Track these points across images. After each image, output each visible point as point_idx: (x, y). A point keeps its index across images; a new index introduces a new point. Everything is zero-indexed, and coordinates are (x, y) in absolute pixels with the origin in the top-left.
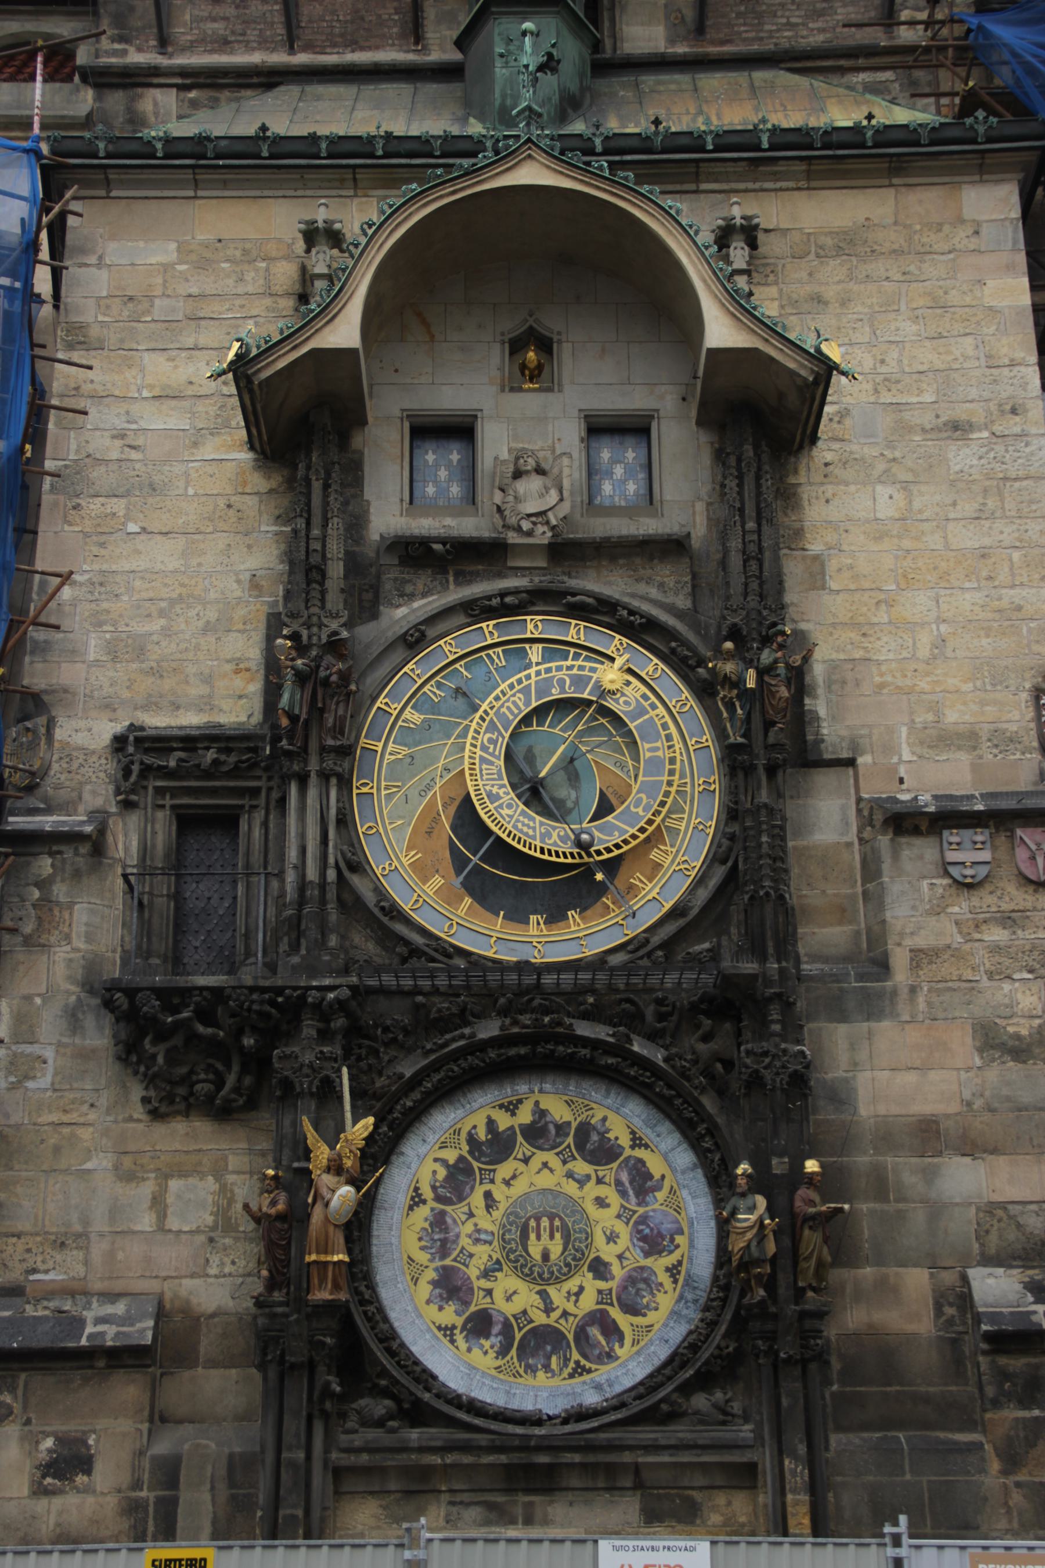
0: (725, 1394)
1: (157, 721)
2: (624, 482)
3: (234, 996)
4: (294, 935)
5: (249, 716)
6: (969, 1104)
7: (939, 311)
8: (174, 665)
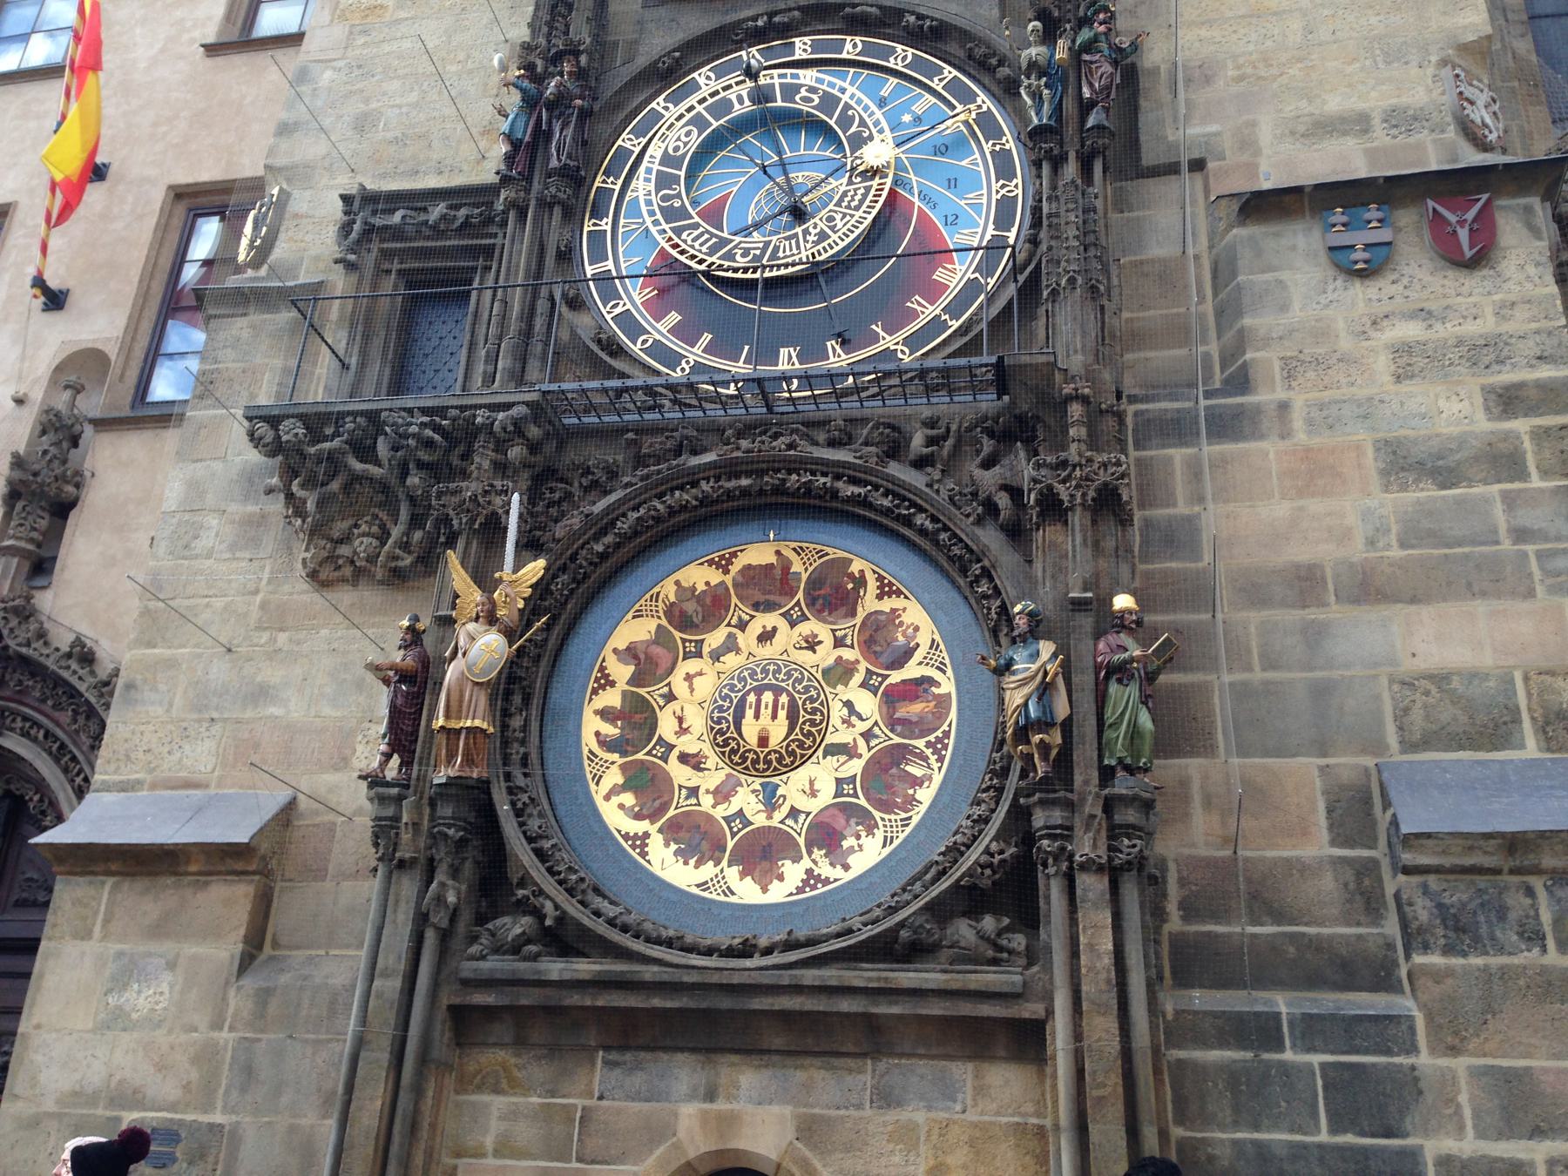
0: (998, 920)
3: (391, 420)
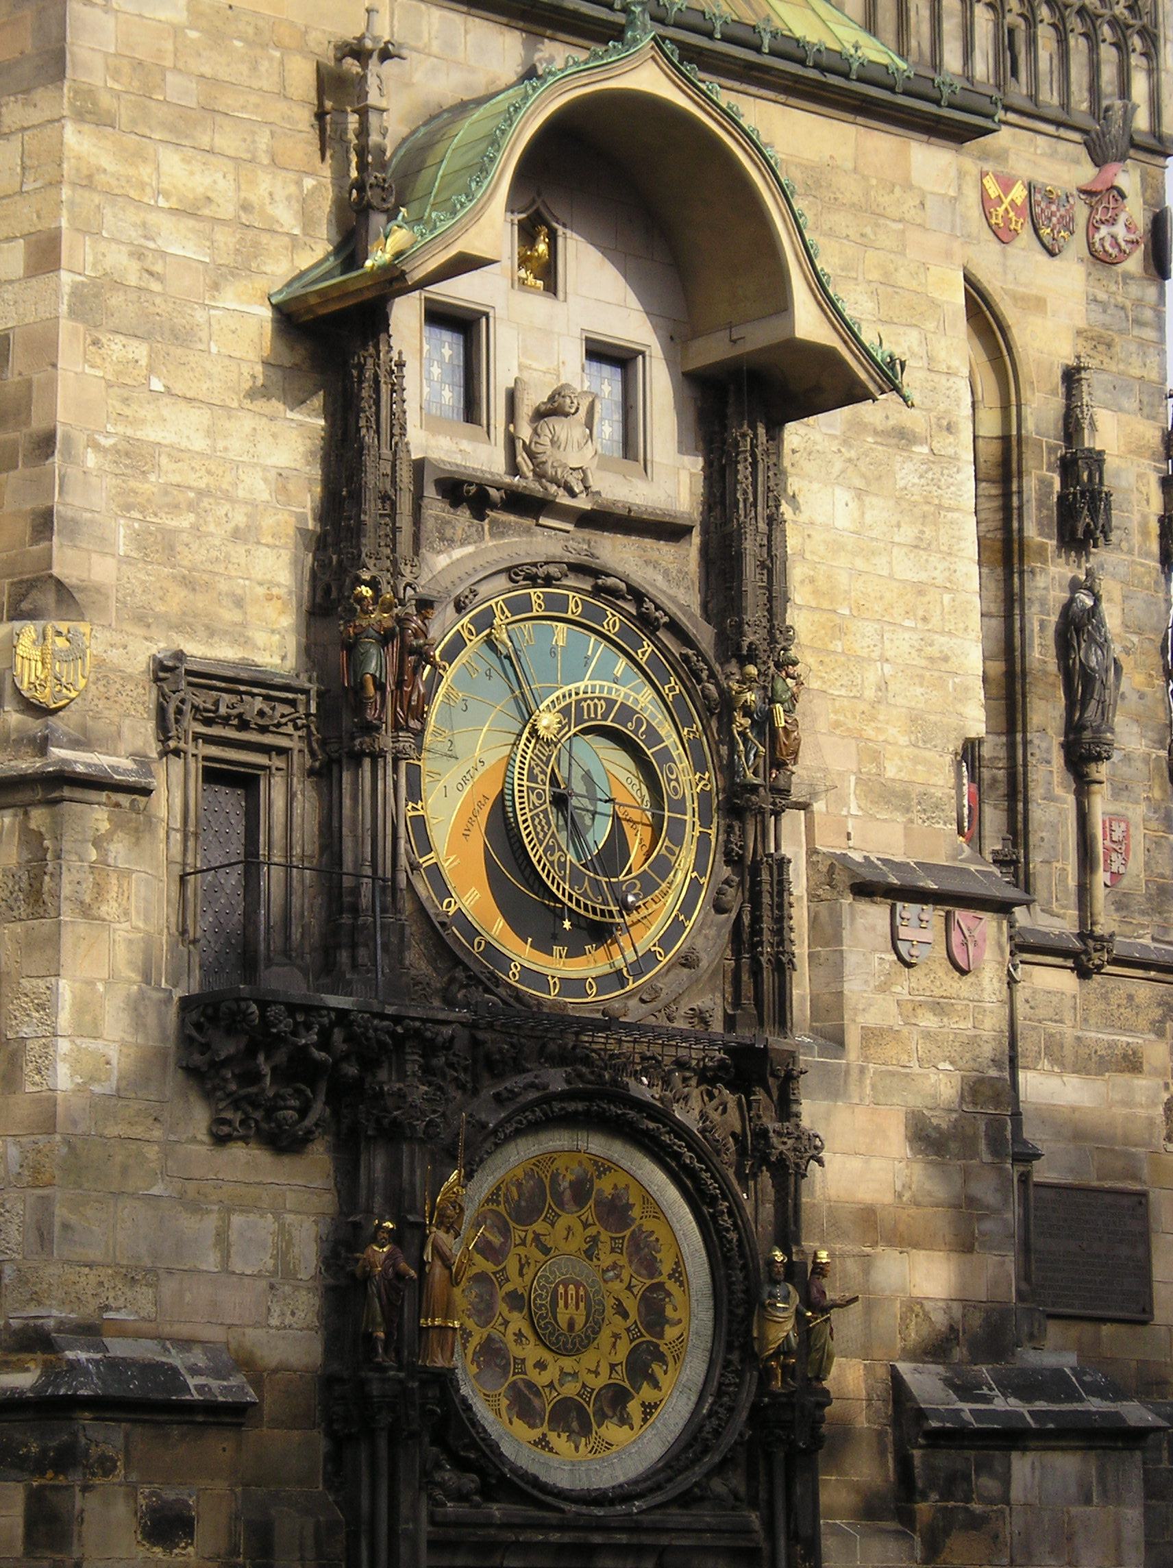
5: (283, 658)
6: (900, 1196)
7: (890, 289)
8: (206, 577)
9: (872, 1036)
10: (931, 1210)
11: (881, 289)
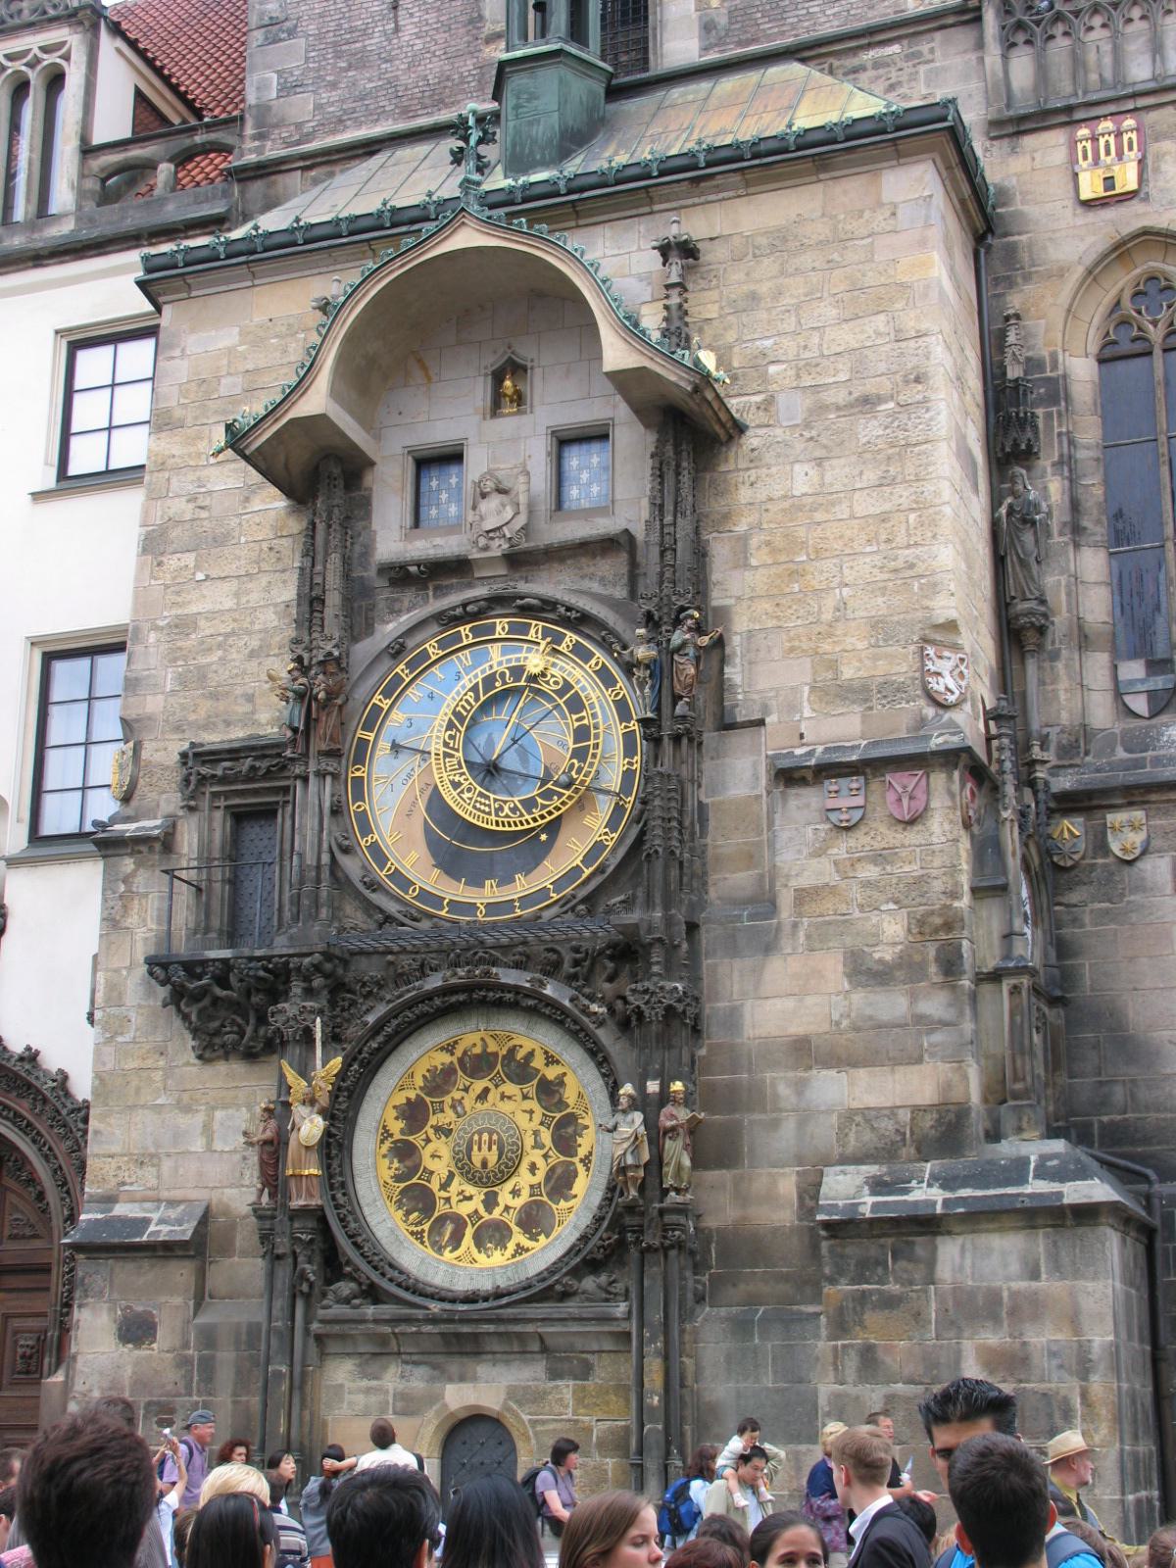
1: (212, 739)
2: (590, 484)
4: (295, 910)
6: (838, 1024)
7: (856, 293)
8: (227, 688)
9: (803, 896)
10: (872, 1032)
11: (846, 296)
